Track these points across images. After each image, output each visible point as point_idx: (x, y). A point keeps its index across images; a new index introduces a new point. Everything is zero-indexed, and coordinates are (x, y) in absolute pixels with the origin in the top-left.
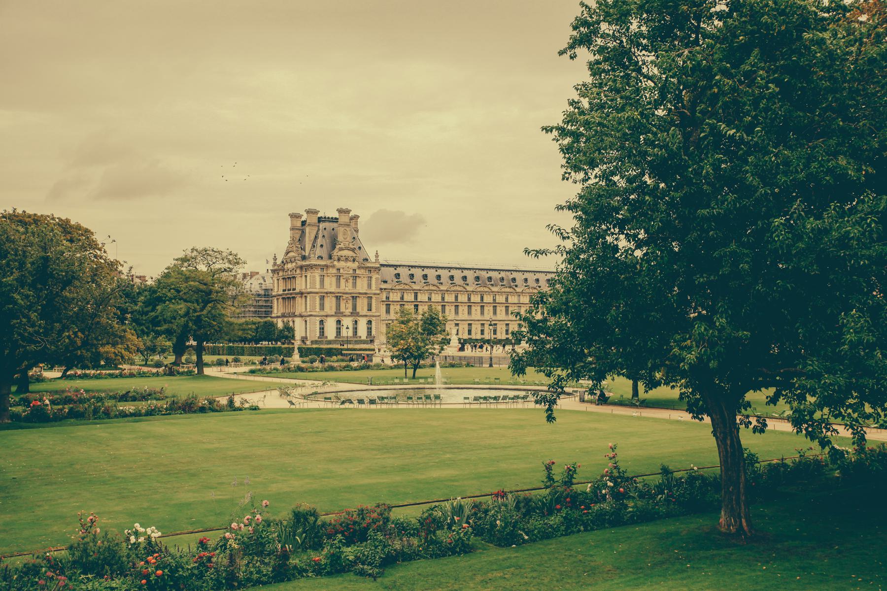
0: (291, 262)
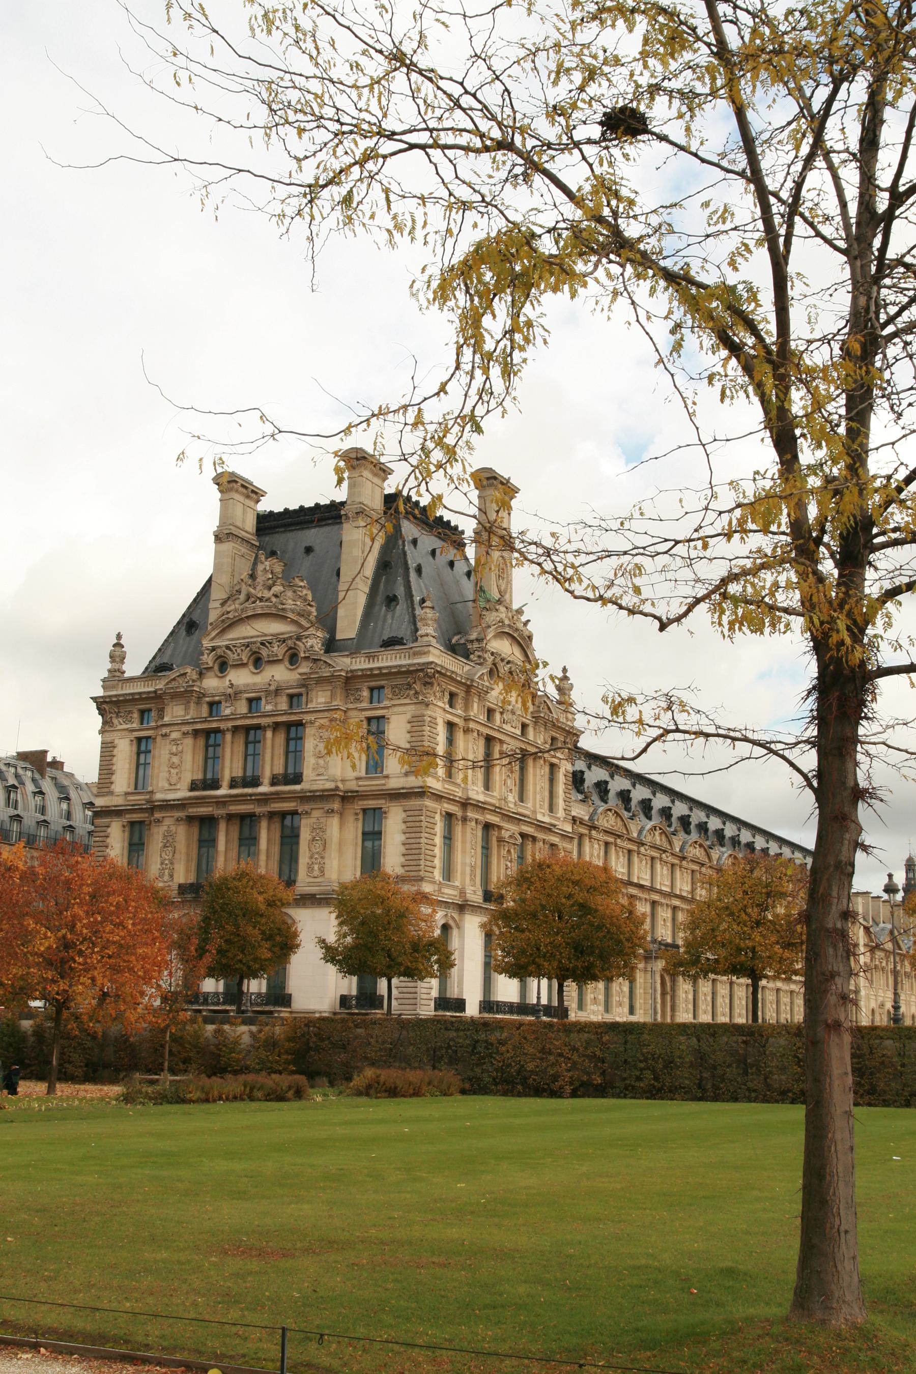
0: (258, 662)
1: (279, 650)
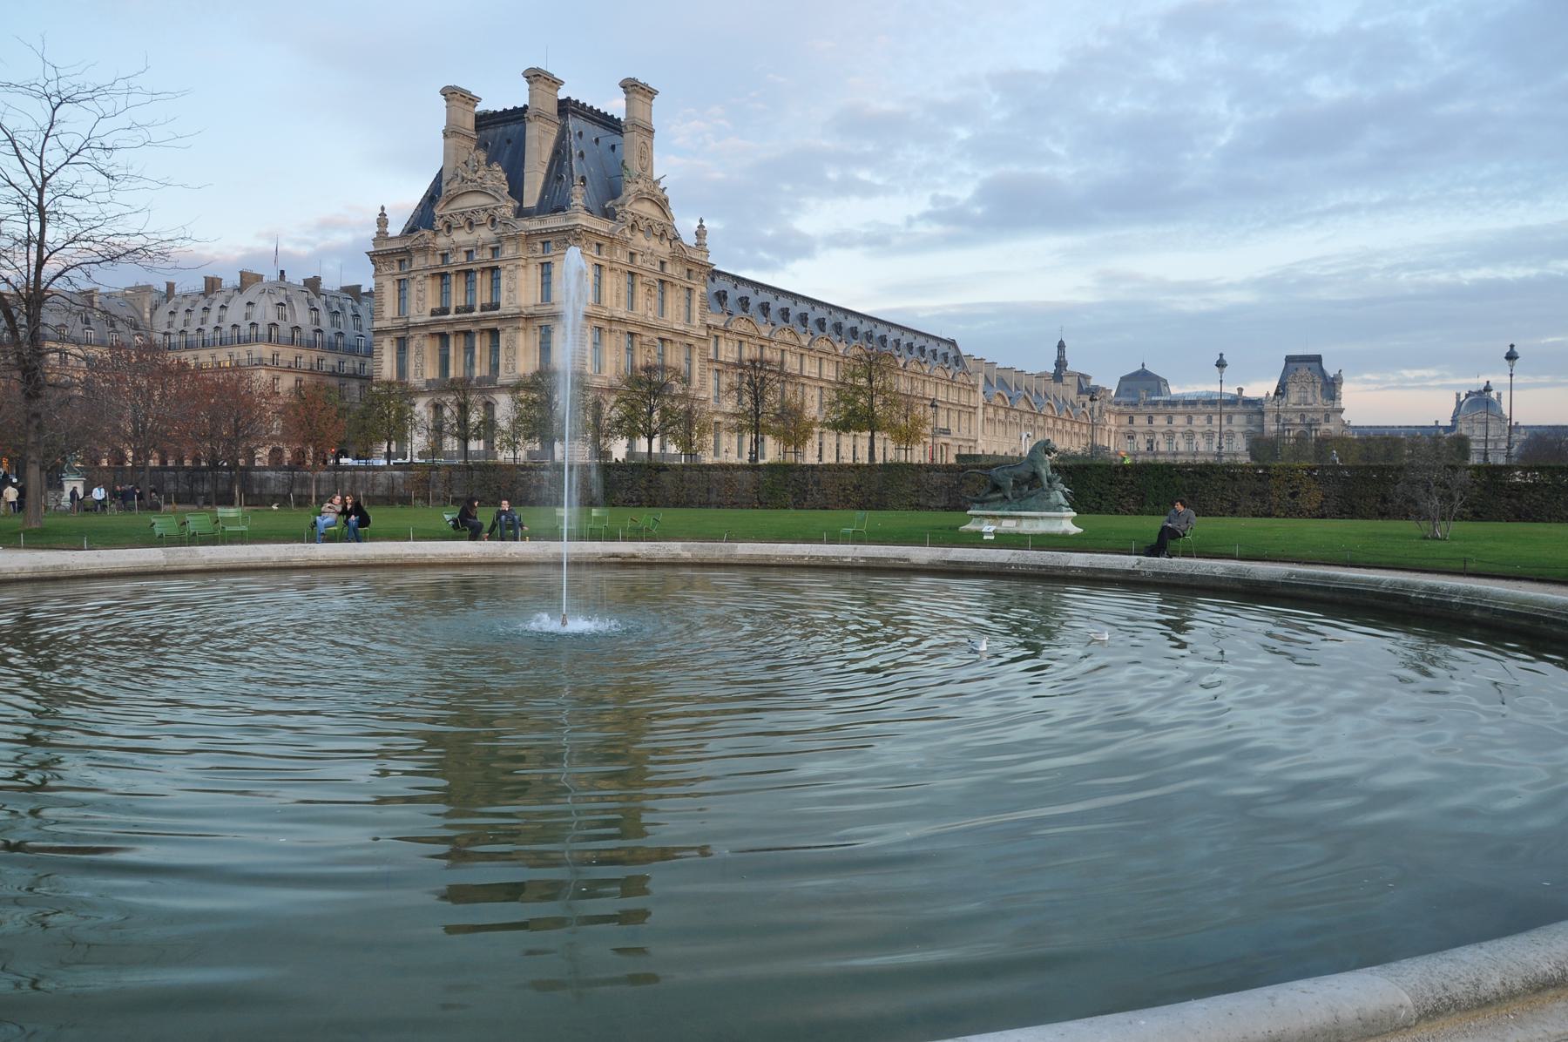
1: (484, 217)
